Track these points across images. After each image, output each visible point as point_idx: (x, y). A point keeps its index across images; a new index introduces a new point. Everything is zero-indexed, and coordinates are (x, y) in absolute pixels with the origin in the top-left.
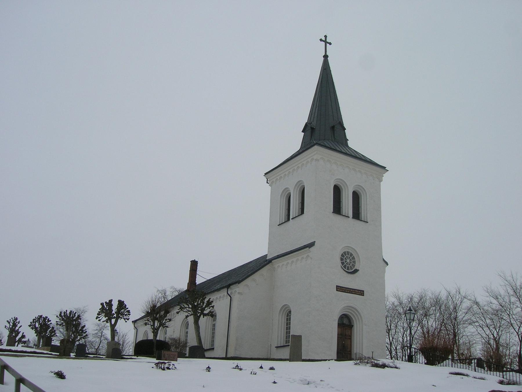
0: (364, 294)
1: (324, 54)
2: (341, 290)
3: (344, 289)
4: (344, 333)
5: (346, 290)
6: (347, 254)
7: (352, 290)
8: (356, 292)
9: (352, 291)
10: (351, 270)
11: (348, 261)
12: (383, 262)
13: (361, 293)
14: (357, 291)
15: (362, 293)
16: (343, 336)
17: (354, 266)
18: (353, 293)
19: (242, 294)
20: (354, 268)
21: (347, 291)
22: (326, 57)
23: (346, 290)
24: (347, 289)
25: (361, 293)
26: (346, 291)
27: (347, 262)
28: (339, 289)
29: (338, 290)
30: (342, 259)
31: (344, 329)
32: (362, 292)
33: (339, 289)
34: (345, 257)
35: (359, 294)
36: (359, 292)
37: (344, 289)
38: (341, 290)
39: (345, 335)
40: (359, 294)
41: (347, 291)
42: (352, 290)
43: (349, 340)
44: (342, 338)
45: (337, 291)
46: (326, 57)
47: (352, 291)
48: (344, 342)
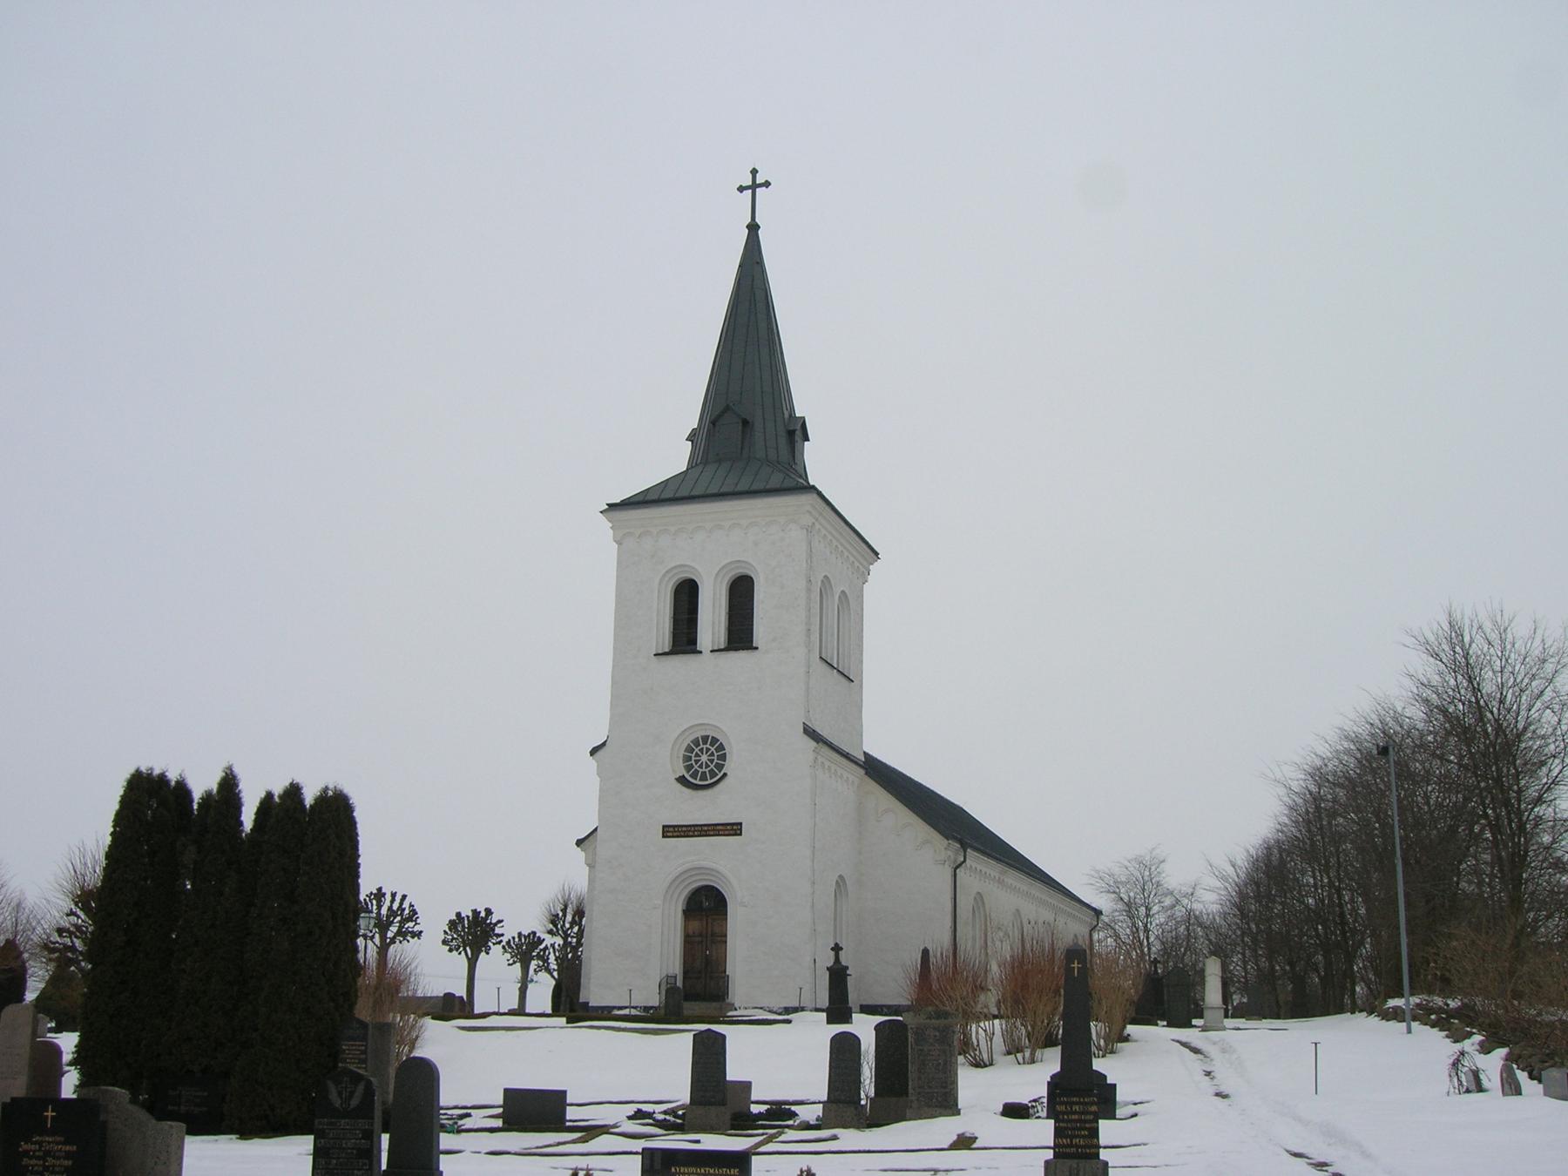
0: (741, 832)
1: (750, 220)
2: (675, 834)
3: (684, 829)
5: (689, 831)
6: (701, 743)
7: (706, 828)
8: (719, 831)
9: (709, 830)
10: (700, 780)
11: (704, 758)
12: (807, 739)
13: (734, 829)
17: (720, 767)
18: (712, 833)
20: (720, 772)
21: (694, 832)
22: (753, 228)
23: (689, 831)
26: (691, 833)
27: (700, 760)
29: (669, 834)
31: (710, 920)
32: (735, 827)
33: (670, 831)
34: (713, 749)
35: (727, 832)
36: (728, 827)
38: (675, 834)
39: (712, 935)
40: (727, 832)
41: (694, 832)
42: (706, 828)
44: (704, 943)
45: (663, 837)
46: (753, 228)
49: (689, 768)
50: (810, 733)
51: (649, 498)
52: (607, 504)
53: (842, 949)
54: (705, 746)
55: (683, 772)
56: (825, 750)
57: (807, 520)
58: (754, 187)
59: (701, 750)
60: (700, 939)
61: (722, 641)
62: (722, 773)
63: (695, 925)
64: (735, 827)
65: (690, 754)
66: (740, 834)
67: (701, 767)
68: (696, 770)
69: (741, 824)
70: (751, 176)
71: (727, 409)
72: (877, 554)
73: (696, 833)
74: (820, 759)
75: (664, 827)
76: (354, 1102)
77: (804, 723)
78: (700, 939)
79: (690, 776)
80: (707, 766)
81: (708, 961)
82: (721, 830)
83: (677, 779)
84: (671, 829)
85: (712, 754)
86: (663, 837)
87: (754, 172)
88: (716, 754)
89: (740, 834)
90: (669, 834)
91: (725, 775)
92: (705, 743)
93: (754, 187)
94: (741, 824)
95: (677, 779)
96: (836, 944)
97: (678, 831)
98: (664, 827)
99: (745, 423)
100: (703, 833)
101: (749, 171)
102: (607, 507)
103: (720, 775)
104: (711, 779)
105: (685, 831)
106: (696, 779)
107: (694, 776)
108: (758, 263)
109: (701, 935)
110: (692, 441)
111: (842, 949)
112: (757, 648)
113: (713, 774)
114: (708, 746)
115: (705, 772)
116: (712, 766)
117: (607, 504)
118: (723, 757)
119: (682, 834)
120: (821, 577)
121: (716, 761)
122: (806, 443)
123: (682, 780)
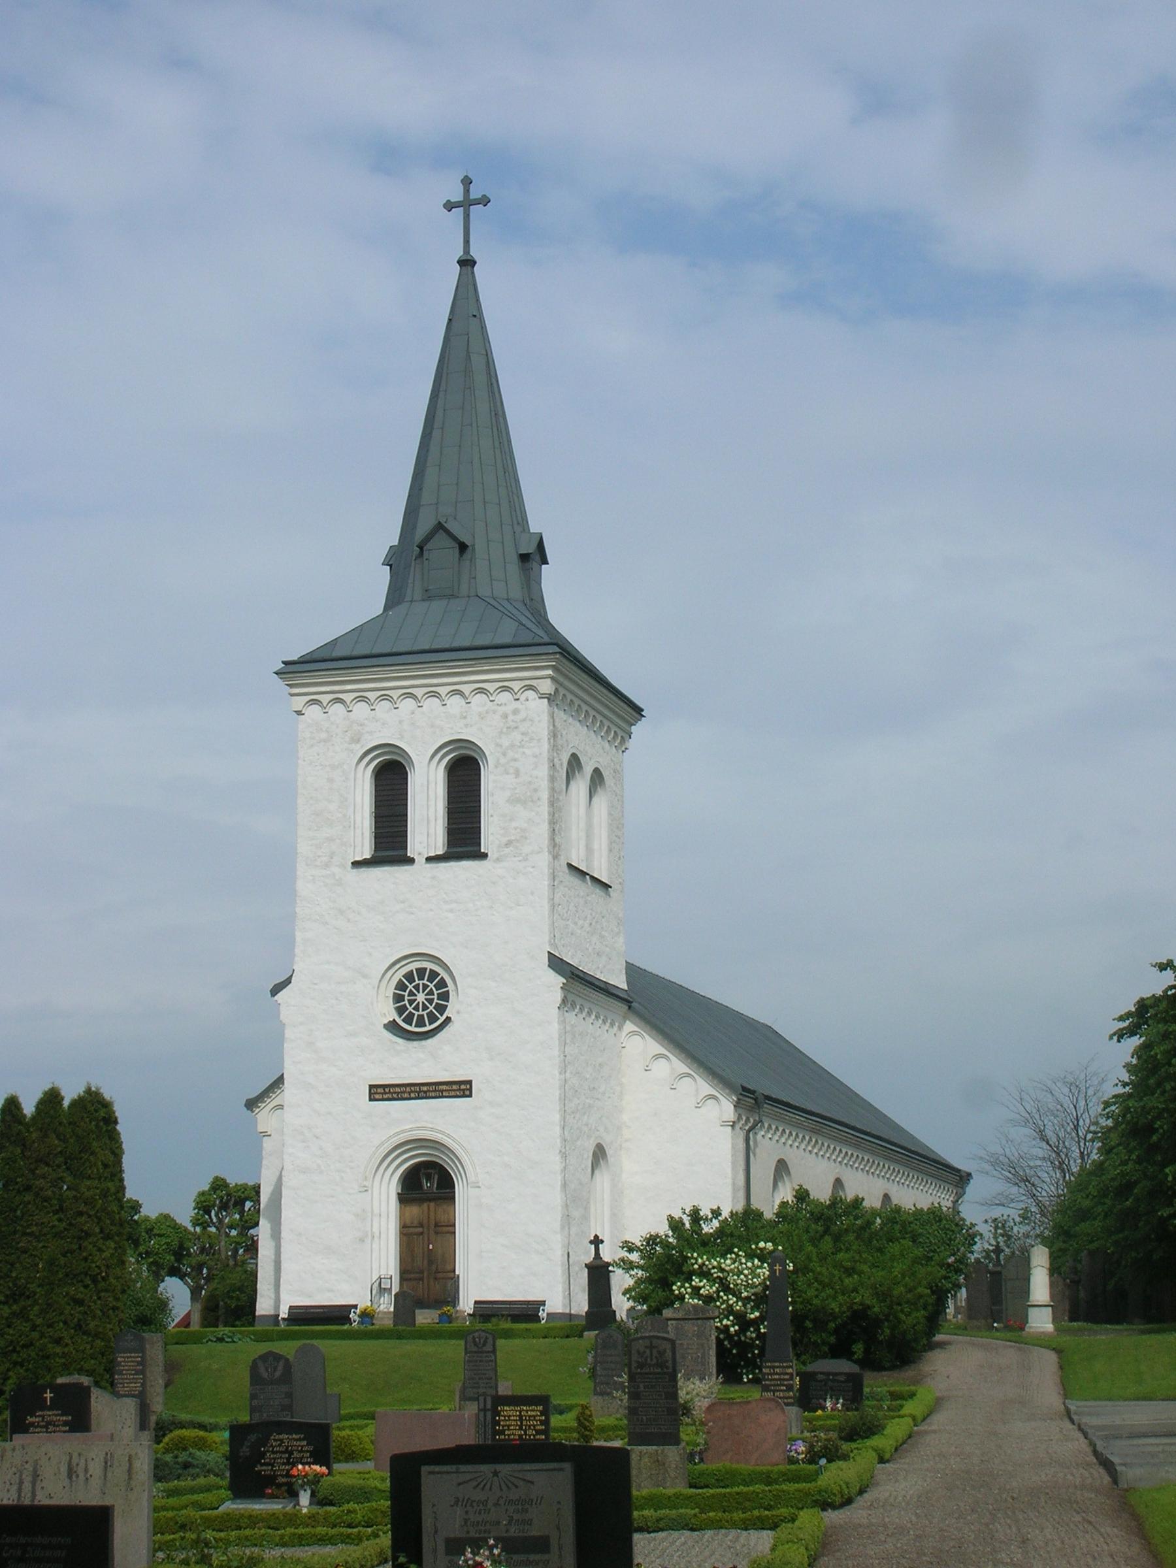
3: (398, 1090)
4: (432, 1217)
5: (404, 1092)
7: (425, 1089)
8: (442, 1091)
9: (429, 1091)
13: (462, 1089)
14: (444, 1087)
15: (464, 1090)
17: (442, 1009)
18: (433, 1094)
19: (270, 1136)
20: (441, 1016)
22: (467, 263)
23: (404, 1092)
24: (408, 1089)
26: (406, 1095)
27: (416, 1000)
29: (377, 1096)
30: (398, 998)
32: (463, 1087)
33: (380, 1092)
35: (453, 1093)
36: (454, 1087)
37: (398, 1090)
39: (436, 1225)
40: (453, 1093)
42: (425, 1089)
44: (426, 1236)
45: (371, 1100)
46: (467, 263)
47: (425, 1092)
48: (431, 1247)
49: (401, 1010)
50: (556, 963)
51: (337, 653)
52: (284, 662)
53: (602, 1242)
54: (421, 982)
55: (393, 1015)
56: (579, 987)
57: (547, 686)
58: (466, 204)
59: (417, 987)
60: (420, 1230)
61: (439, 846)
62: (444, 1017)
63: (414, 1211)
64: (463, 1087)
65: (403, 993)
66: (470, 1096)
67: (416, 1008)
68: (410, 1012)
69: (470, 1082)
70: (462, 187)
71: (440, 527)
72: (638, 710)
73: (413, 1095)
74: (571, 997)
75: (371, 1087)
76: (278, 1374)
77: (549, 952)
78: (420, 1230)
79: (403, 1020)
80: (425, 1008)
81: (431, 1257)
82: (445, 1090)
83: (386, 1026)
84: (380, 1090)
85: (431, 993)
86: (371, 1100)
87: (467, 182)
88: (436, 992)
89: (470, 1096)
90: (377, 1096)
91: (448, 1020)
92: (421, 978)
93: (466, 204)
94: (470, 1082)
95: (386, 1026)
96: (596, 1237)
97: (390, 1092)
98: (371, 1087)
99: (463, 547)
100: (422, 1094)
101: (460, 181)
102: (283, 665)
103: (442, 1019)
104: (430, 1024)
105: (398, 1093)
106: (411, 1025)
107: (408, 1020)
108: (475, 316)
109: (421, 1225)
110: (391, 566)
111: (602, 1242)
112: (484, 856)
113: (433, 1019)
114: (425, 982)
115: (423, 1015)
116: (431, 1008)
117: (284, 662)
118: (445, 996)
119: (395, 1096)
120: (565, 758)
121: (436, 1001)
122: (543, 566)
123: (392, 1027)
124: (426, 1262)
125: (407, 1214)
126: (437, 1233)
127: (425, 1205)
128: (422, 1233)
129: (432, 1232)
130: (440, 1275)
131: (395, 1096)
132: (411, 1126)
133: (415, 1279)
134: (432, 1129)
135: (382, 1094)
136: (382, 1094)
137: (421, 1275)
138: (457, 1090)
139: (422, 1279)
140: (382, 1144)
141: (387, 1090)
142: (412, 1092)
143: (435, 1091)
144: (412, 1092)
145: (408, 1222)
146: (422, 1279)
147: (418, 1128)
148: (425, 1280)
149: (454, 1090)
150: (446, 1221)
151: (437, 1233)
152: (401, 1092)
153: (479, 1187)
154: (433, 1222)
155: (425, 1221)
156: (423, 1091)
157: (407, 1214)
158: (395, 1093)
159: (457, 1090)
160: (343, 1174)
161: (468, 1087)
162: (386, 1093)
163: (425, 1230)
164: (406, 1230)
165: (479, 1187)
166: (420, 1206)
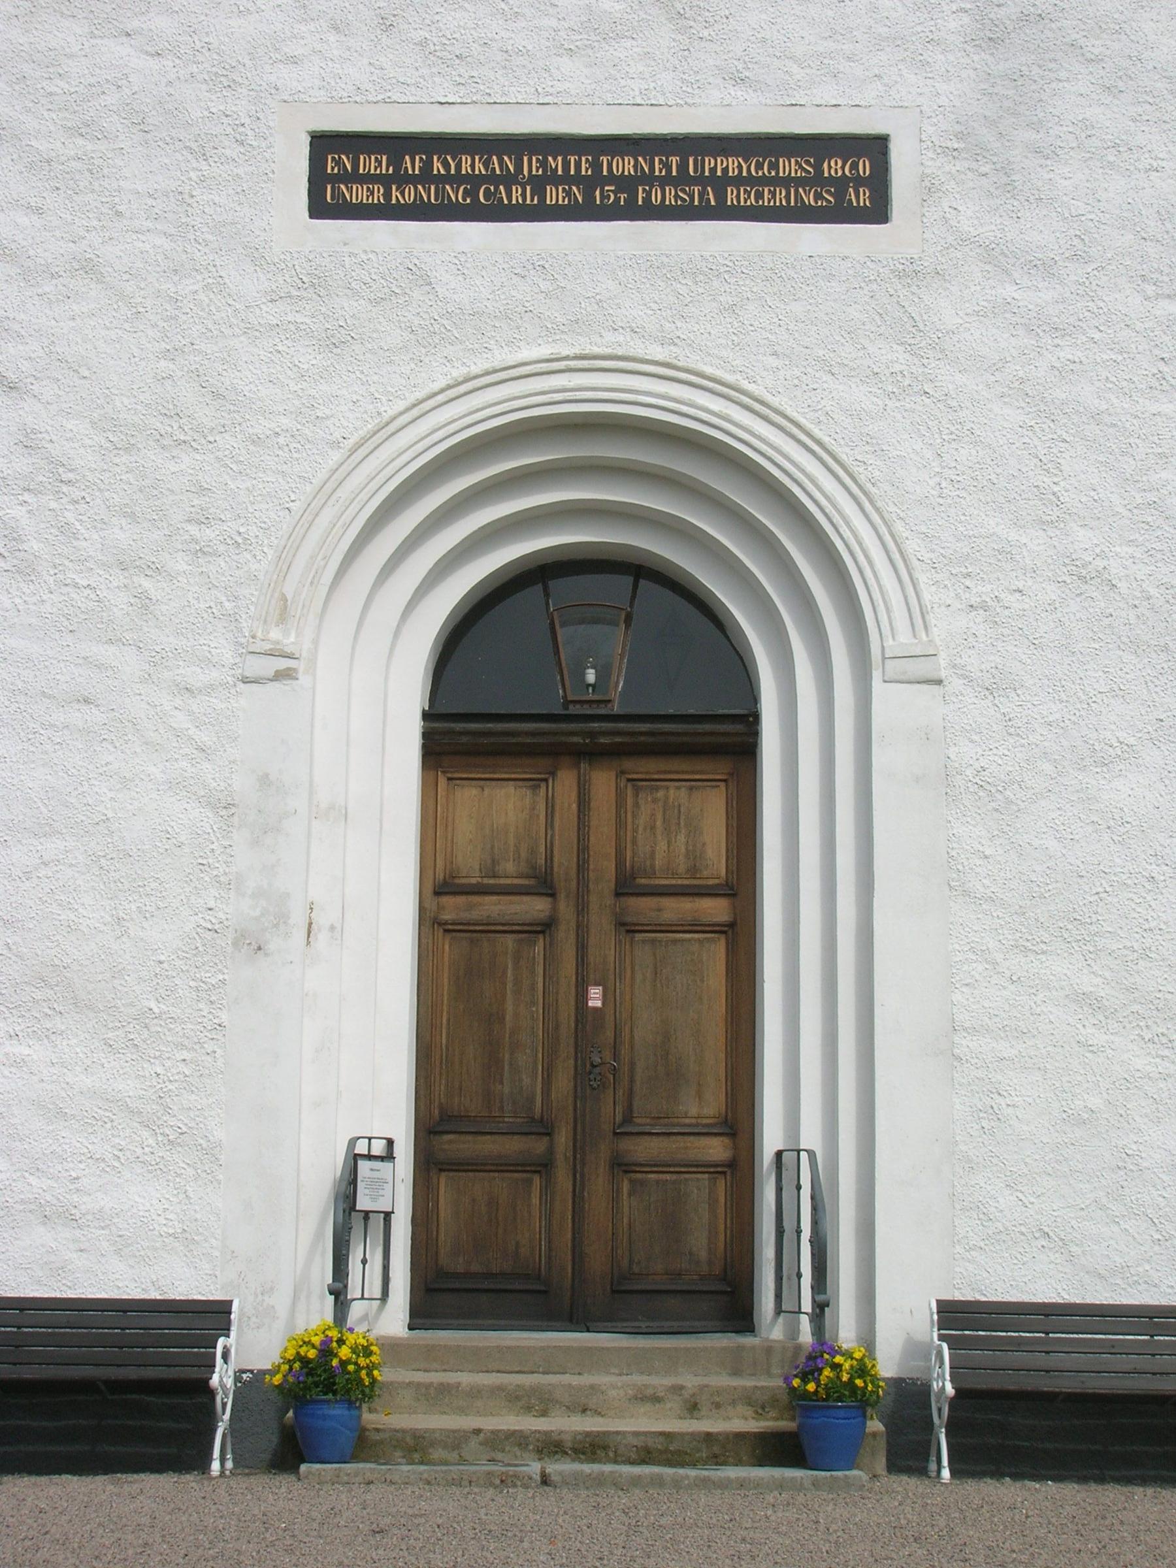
3: (469, 164)
5: (509, 180)
7: (625, 166)
8: (721, 183)
9: (648, 179)
14: (732, 165)
15: (840, 185)
16: (582, 908)
24: (531, 166)
25: (817, 180)
28: (368, 179)
29: (358, 194)
32: (834, 167)
36: (788, 167)
37: (469, 164)
41: (538, 185)
42: (625, 166)
43: (716, 952)
44: (566, 936)
45: (319, 208)
47: (626, 184)
48: (595, 998)
60: (537, 907)
64: (834, 167)
66: (878, 212)
73: (555, 196)
78: (537, 907)
82: (738, 181)
84: (369, 164)
86: (319, 208)
89: (878, 212)
90: (358, 194)
97: (426, 178)
105: (475, 181)
119: (457, 195)
124: (563, 1083)
125: (465, 829)
126: (627, 928)
127: (565, 783)
128: (545, 927)
129: (601, 922)
130: (644, 1149)
131: (457, 195)
132: (545, 351)
133: (501, 1166)
134: (669, 372)
135: (385, 181)
136: (385, 181)
137: (539, 1146)
138: (800, 182)
139: (544, 1166)
140: (386, 429)
141: (412, 165)
142: (552, 179)
143: (683, 179)
144: (552, 179)
145: (470, 866)
146: (544, 1166)
147: (587, 362)
148: (563, 1178)
149: (786, 182)
150: (682, 865)
151: (627, 928)
152: (492, 179)
153: (939, 682)
154: (604, 868)
155: (564, 862)
156: (612, 178)
157: (465, 829)
158: (458, 179)
159: (800, 182)
160: (146, 584)
161: (865, 168)
162: (403, 179)
163: (566, 910)
164: (453, 908)
165: (939, 682)
166: (535, 784)
